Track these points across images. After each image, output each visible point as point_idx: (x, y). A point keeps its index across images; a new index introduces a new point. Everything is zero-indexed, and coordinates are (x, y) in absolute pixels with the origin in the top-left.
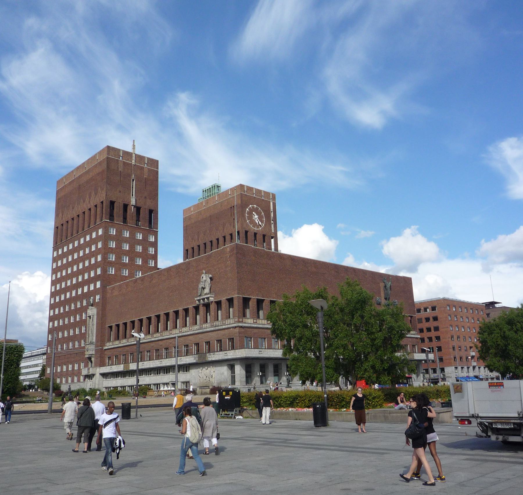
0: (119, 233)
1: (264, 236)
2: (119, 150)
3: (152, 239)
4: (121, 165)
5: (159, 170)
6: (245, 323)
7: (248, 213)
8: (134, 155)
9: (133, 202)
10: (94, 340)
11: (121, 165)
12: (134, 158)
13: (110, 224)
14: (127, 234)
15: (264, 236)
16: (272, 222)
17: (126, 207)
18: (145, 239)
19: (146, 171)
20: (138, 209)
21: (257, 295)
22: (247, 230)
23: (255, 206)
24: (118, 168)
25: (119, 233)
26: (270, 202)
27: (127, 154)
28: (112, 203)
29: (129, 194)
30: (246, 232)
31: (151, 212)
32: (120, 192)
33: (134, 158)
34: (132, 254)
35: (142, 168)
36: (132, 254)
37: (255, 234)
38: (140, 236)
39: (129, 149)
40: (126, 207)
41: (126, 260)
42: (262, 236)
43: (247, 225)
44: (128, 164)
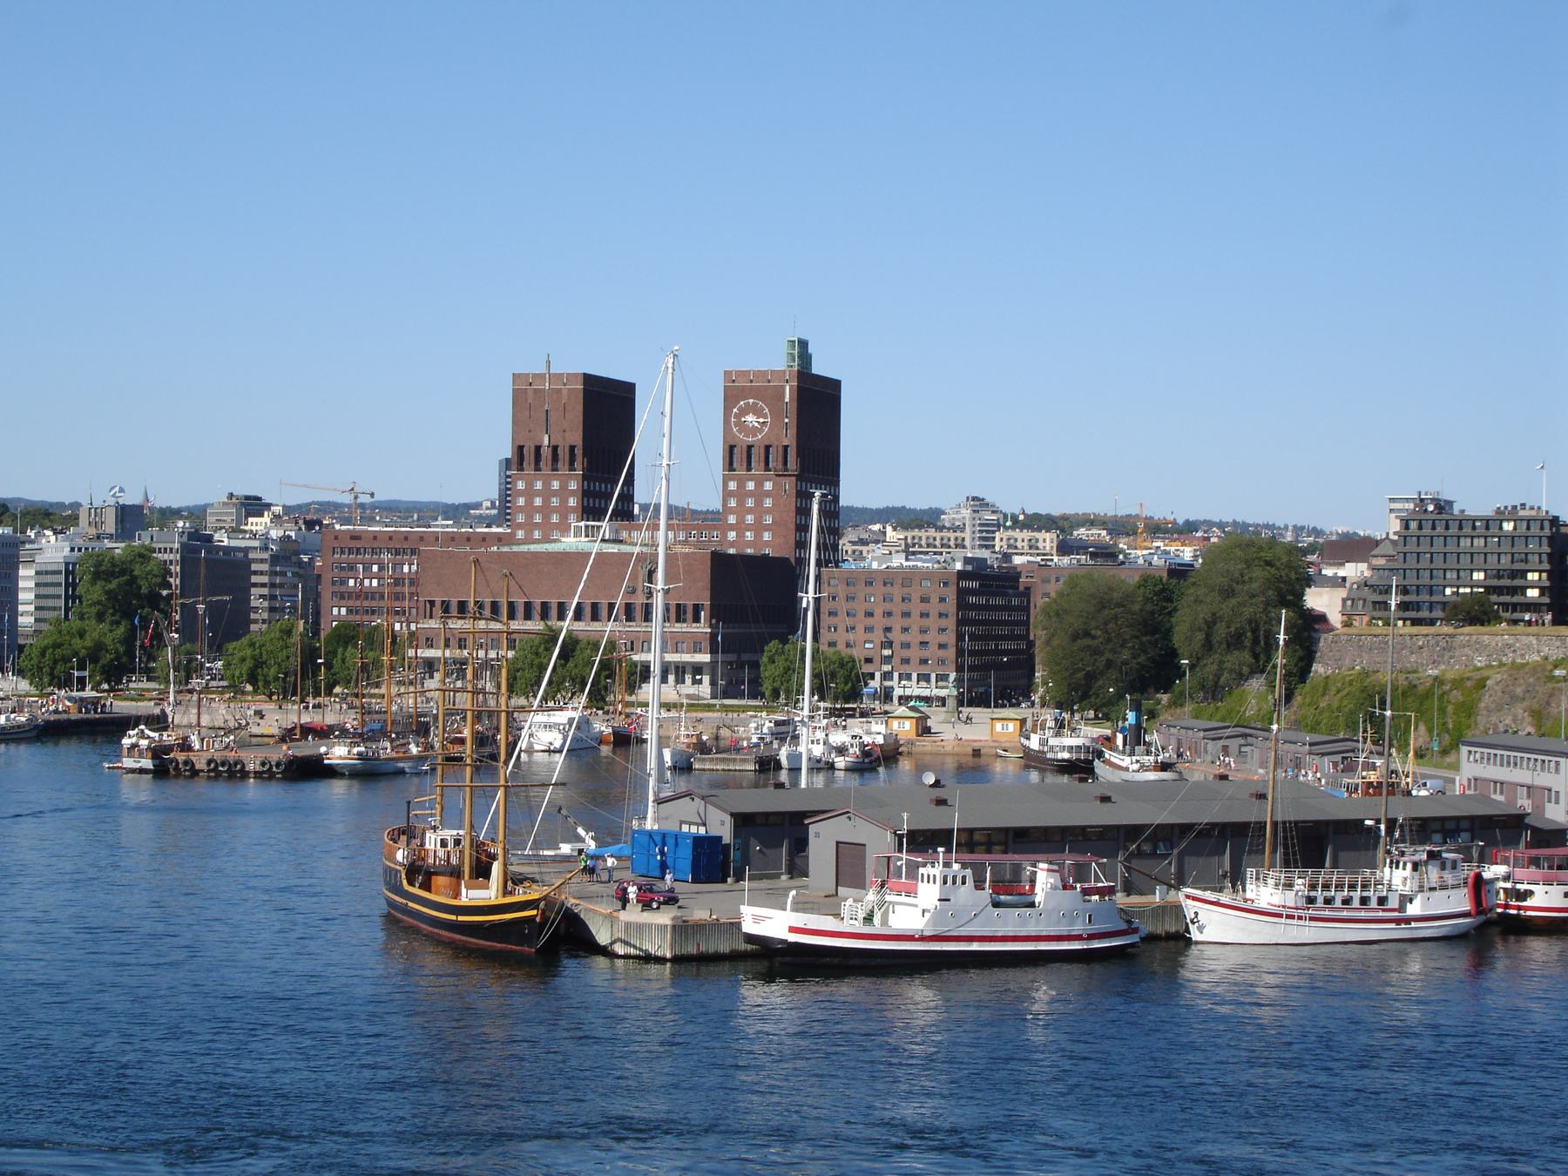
0: (530, 485)
1: (767, 448)
7: (737, 416)
9: (546, 442)
14: (539, 485)
15: (767, 448)
18: (564, 487)
20: (555, 448)
25: (530, 485)
26: (783, 388)
27: (542, 376)
28: (521, 448)
34: (546, 510)
36: (546, 510)
38: (556, 485)
39: (542, 370)
40: (538, 448)
41: (538, 519)
43: (734, 436)
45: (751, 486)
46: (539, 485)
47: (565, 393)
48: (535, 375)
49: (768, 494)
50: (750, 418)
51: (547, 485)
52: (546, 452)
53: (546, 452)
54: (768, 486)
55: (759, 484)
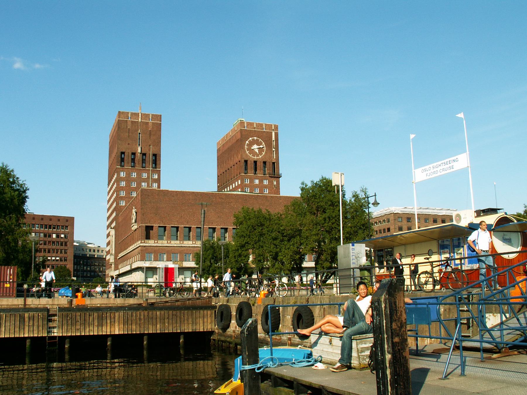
0: (129, 175)
2: (128, 113)
3: (156, 177)
4: (129, 123)
5: (162, 122)
6: (146, 243)
8: (140, 114)
10: (114, 253)
11: (129, 123)
12: (140, 117)
13: (121, 169)
14: (134, 175)
15: (265, 163)
16: (274, 149)
17: (134, 154)
19: (150, 125)
21: (159, 223)
22: (246, 159)
23: (255, 138)
24: (127, 126)
25: (129, 175)
29: (136, 145)
30: (246, 162)
31: (155, 155)
32: (129, 144)
33: (140, 117)
35: (147, 123)
37: (255, 162)
42: (262, 164)
43: (247, 155)
44: (135, 122)
45: (257, 182)
46: (134, 175)
47: (150, 125)
48: (132, 114)
49: (266, 187)
50: (255, 147)
51: (139, 175)
52: (139, 156)
53: (139, 156)
54: (266, 182)
55: (261, 181)
